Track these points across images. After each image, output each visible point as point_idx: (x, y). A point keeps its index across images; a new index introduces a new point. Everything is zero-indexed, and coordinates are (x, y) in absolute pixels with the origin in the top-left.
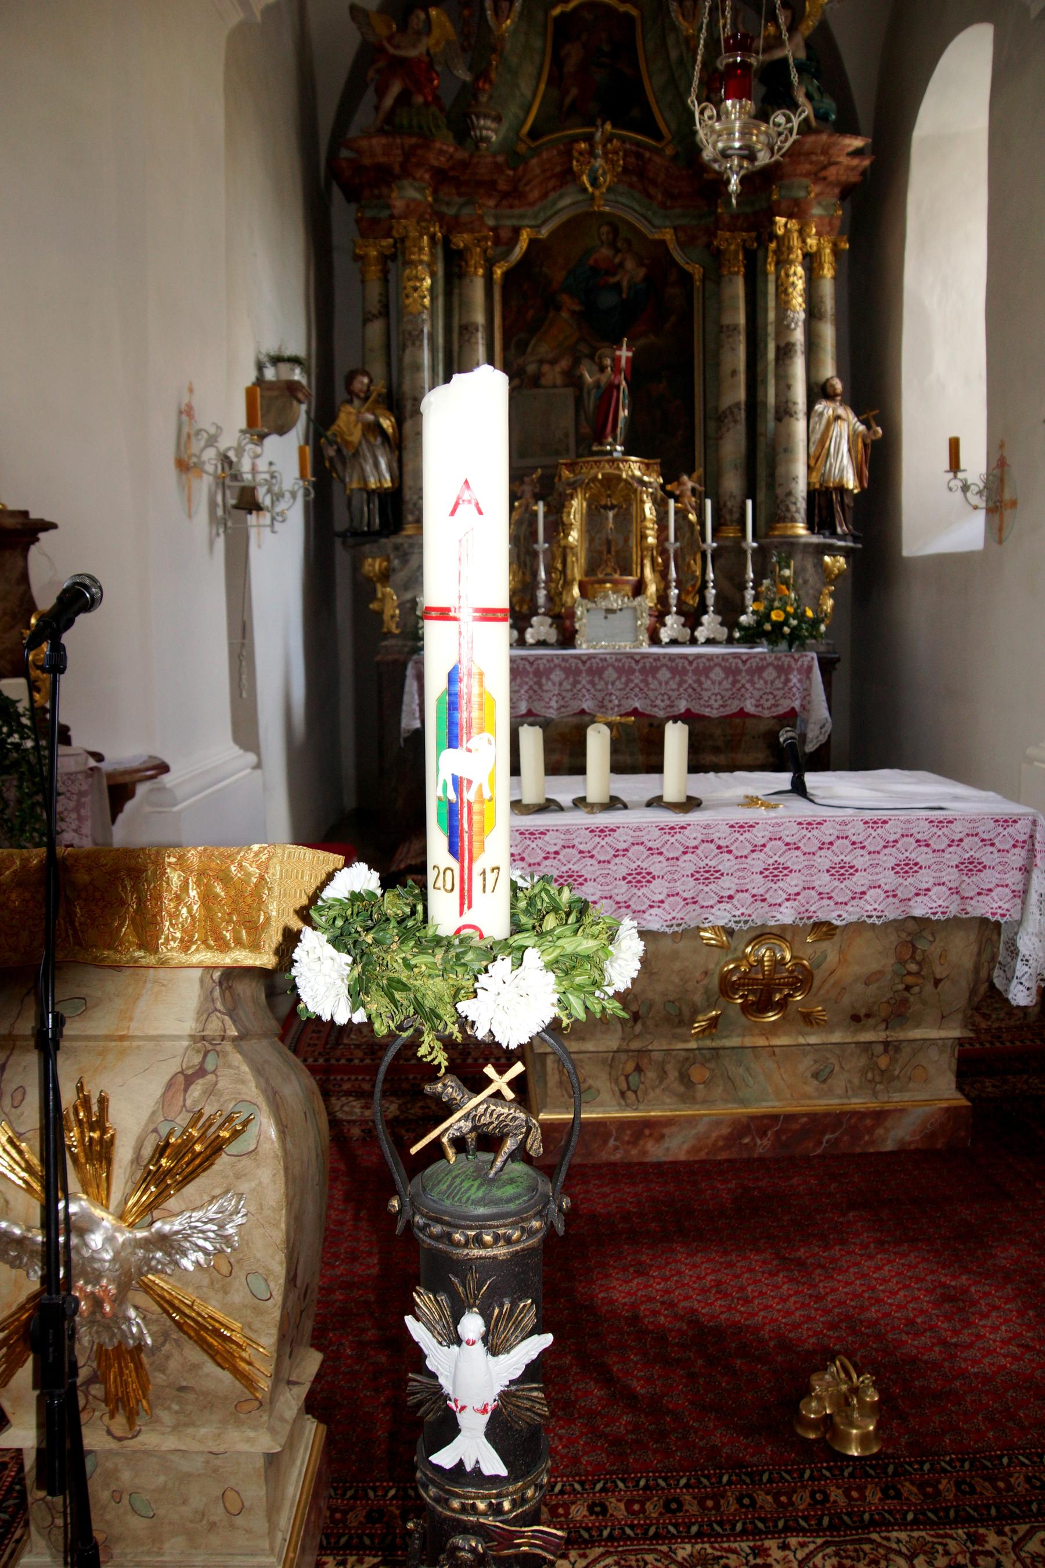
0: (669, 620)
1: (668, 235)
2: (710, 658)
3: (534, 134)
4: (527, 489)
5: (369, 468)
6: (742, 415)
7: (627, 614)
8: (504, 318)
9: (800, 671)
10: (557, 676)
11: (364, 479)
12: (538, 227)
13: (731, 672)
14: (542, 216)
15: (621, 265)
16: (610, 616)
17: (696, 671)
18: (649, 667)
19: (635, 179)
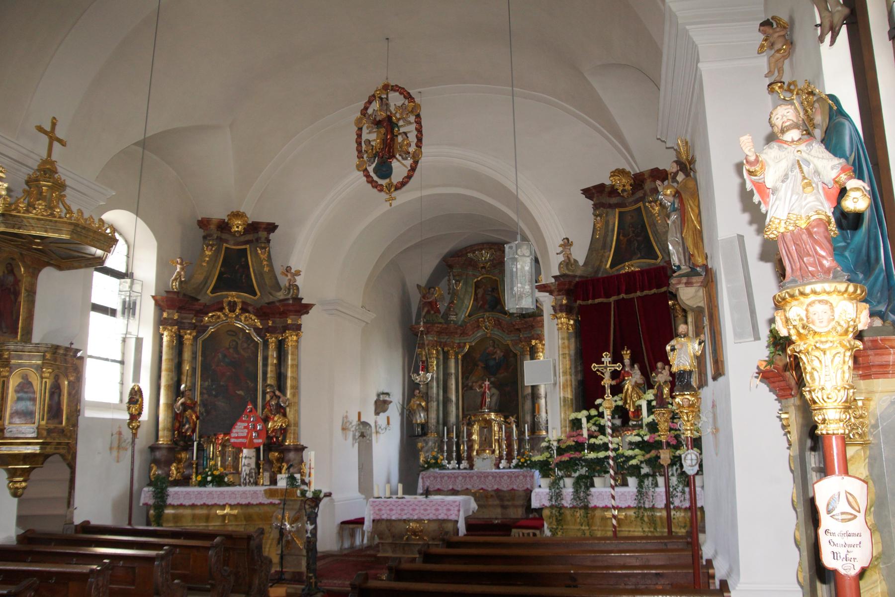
0: (502, 461)
1: (509, 342)
2: (503, 473)
3: (469, 316)
4: (465, 422)
5: (418, 417)
6: (530, 397)
7: (489, 460)
8: (462, 369)
9: (530, 476)
10: (460, 478)
11: (416, 420)
12: (471, 342)
13: (510, 477)
14: (473, 339)
15: (496, 352)
16: (484, 461)
17: (500, 477)
18: (494, 476)
19: (499, 327)
